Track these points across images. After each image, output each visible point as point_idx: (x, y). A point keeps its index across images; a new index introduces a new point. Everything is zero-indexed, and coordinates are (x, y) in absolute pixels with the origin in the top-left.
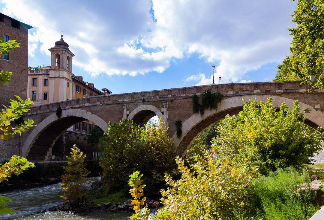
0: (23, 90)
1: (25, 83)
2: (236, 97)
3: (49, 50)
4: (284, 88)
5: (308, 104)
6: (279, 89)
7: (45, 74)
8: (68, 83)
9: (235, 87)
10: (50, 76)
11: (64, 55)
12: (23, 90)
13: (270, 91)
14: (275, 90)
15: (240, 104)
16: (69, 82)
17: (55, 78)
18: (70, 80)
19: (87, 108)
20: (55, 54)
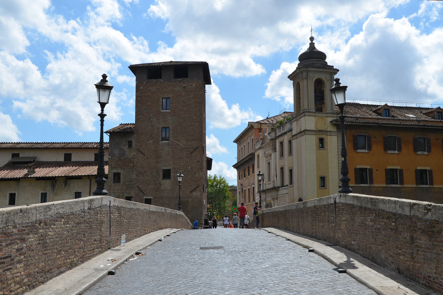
0: (195, 189)
1: (197, 174)
10: (294, 132)
11: (305, 81)
12: (195, 189)
16: (323, 136)
17: (298, 136)
18: (329, 130)
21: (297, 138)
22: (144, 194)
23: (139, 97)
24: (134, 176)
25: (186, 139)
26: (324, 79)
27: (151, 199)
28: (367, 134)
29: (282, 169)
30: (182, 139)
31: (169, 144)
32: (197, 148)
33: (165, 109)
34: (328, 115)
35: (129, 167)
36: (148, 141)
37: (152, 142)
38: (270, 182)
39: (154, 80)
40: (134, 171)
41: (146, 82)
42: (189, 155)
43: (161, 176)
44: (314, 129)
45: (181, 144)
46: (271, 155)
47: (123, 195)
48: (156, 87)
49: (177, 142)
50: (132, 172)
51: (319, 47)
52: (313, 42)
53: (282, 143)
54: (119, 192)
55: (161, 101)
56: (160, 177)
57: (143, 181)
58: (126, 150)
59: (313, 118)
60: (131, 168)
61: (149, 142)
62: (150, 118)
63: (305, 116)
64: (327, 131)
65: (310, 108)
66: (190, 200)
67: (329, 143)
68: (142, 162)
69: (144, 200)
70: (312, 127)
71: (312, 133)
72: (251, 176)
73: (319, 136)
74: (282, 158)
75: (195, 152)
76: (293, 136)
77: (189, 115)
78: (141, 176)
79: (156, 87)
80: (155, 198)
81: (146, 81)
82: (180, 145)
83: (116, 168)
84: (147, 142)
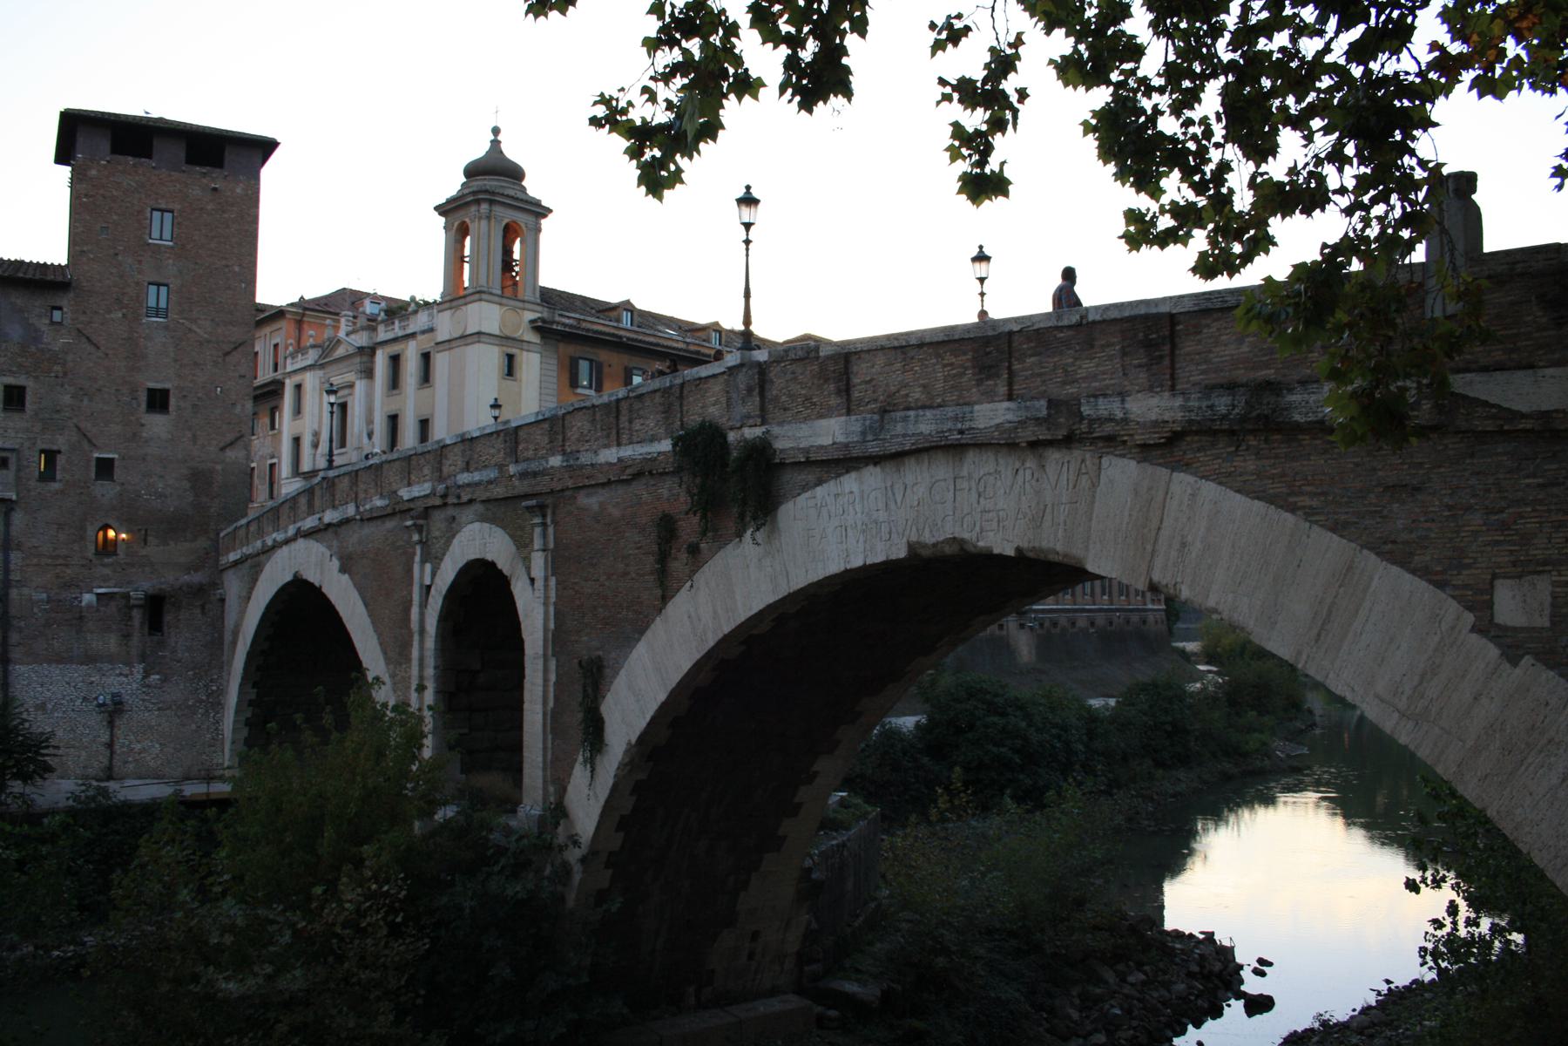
0: (232, 444)
2: (872, 477)
3: (436, 213)
4: (1190, 373)
5: (1422, 572)
6: (1151, 389)
7: (423, 332)
8: (510, 358)
9: (861, 372)
10: (442, 335)
12: (232, 444)
13: (1086, 410)
14: (1123, 395)
15: (894, 536)
17: (454, 344)
18: (526, 338)
19: (329, 534)
20: (456, 224)
21: (450, 349)
22: (95, 445)
23: (86, 196)
24: (67, 399)
25: (212, 320)
26: (523, 226)
27: (113, 459)
28: (595, 358)
29: (393, 420)
30: (202, 317)
31: (166, 327)
32: (240, 345)
33: (158, 237)
34: (528, 306)
35: (53, 375)
36: (110, 312)
37: (120, 315)
38: (343, 450)
39: (130, 158)
40: (66, 386)
41: (108, 162)
42: (220, 360)
43: (144, 406)
44: (497, 332)
45: (198, 330)
46: (351, 386)
47: (34, 444)
48: (137, 178)
49: (187, 323)
50: (62, 386)
51: (512, 151)
52: (499, 138)
53: (395, 360)
54: (20, 435)
55: (149, 215)
56: (139, 405)
57: (92, 414)
58: (44, 328)
59: (497, 307)
60: (57, 377)
61: (112, 316)
62: (117, 254)
63: (481, 300)
64: (523, 341)
65: (491, 284)
66: (219, 467)
67: (524, 366)
68: (91, 365)
69: (93, 463)
70: (493, 327)
71: (492, 341)
72: (265, 437)
73: (505, 349)
74: (395, 392)
75: (234, 353)
76: (437, 344)
77: (224, 262)
78: (86, 402)
79: (137, 178)
80: (124, 459)
81: (108, 159)
82: (195, 332)
83: (14, 373)
84: (107, 316)
